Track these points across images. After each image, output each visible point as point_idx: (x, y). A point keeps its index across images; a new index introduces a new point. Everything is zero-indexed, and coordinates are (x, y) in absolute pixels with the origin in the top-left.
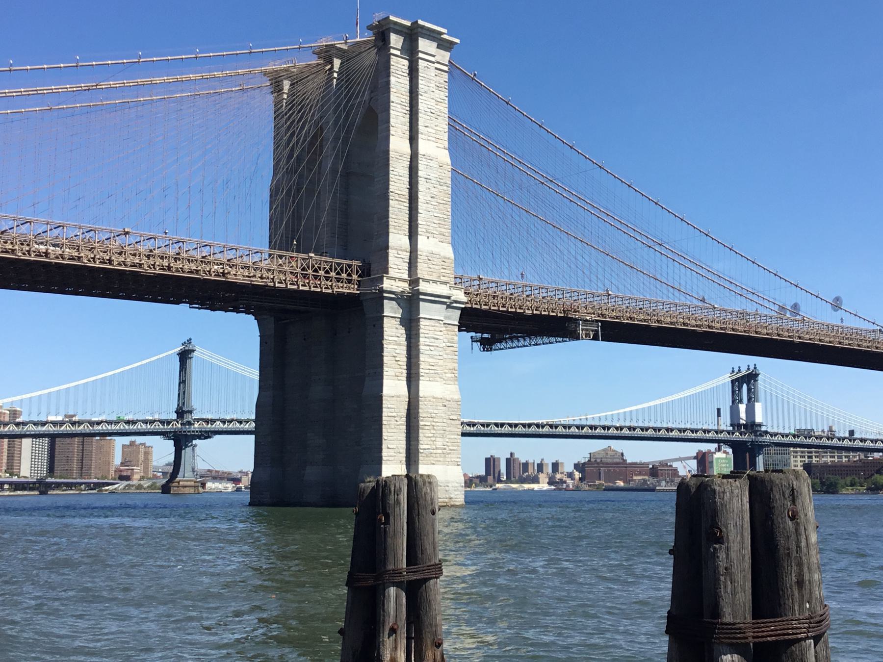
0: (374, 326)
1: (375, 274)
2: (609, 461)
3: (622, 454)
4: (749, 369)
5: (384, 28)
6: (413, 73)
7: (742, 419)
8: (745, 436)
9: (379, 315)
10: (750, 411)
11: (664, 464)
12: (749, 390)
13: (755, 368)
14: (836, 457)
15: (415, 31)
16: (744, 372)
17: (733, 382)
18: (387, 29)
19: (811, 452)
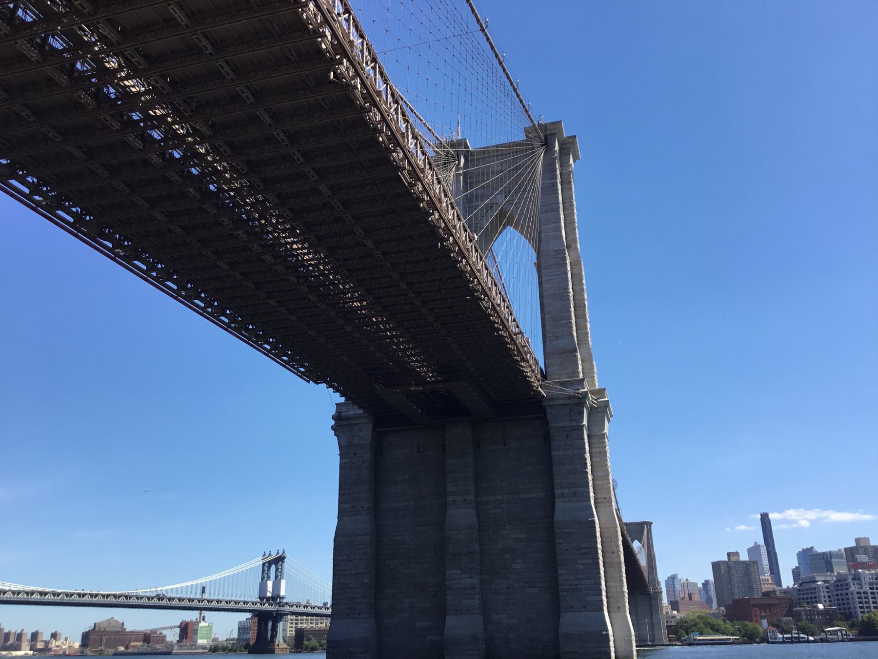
0: (567, 436)
1: (554, 379)
2: (111, 629)
3: (123, 624)
4: (278, 553)
5: (549, 132)
6: (566, 183)
7: (270, 592)
8: (272, 606)
9: (574, 423)
10: (277, 586)
11: (154, 632)
12: (277, 569)
13: (284, 552)
14: (314, 623)
15: (568, 146)
16: (274, 556)
17: (264, 564)
18: (551, 134)
19: (297, 620)
